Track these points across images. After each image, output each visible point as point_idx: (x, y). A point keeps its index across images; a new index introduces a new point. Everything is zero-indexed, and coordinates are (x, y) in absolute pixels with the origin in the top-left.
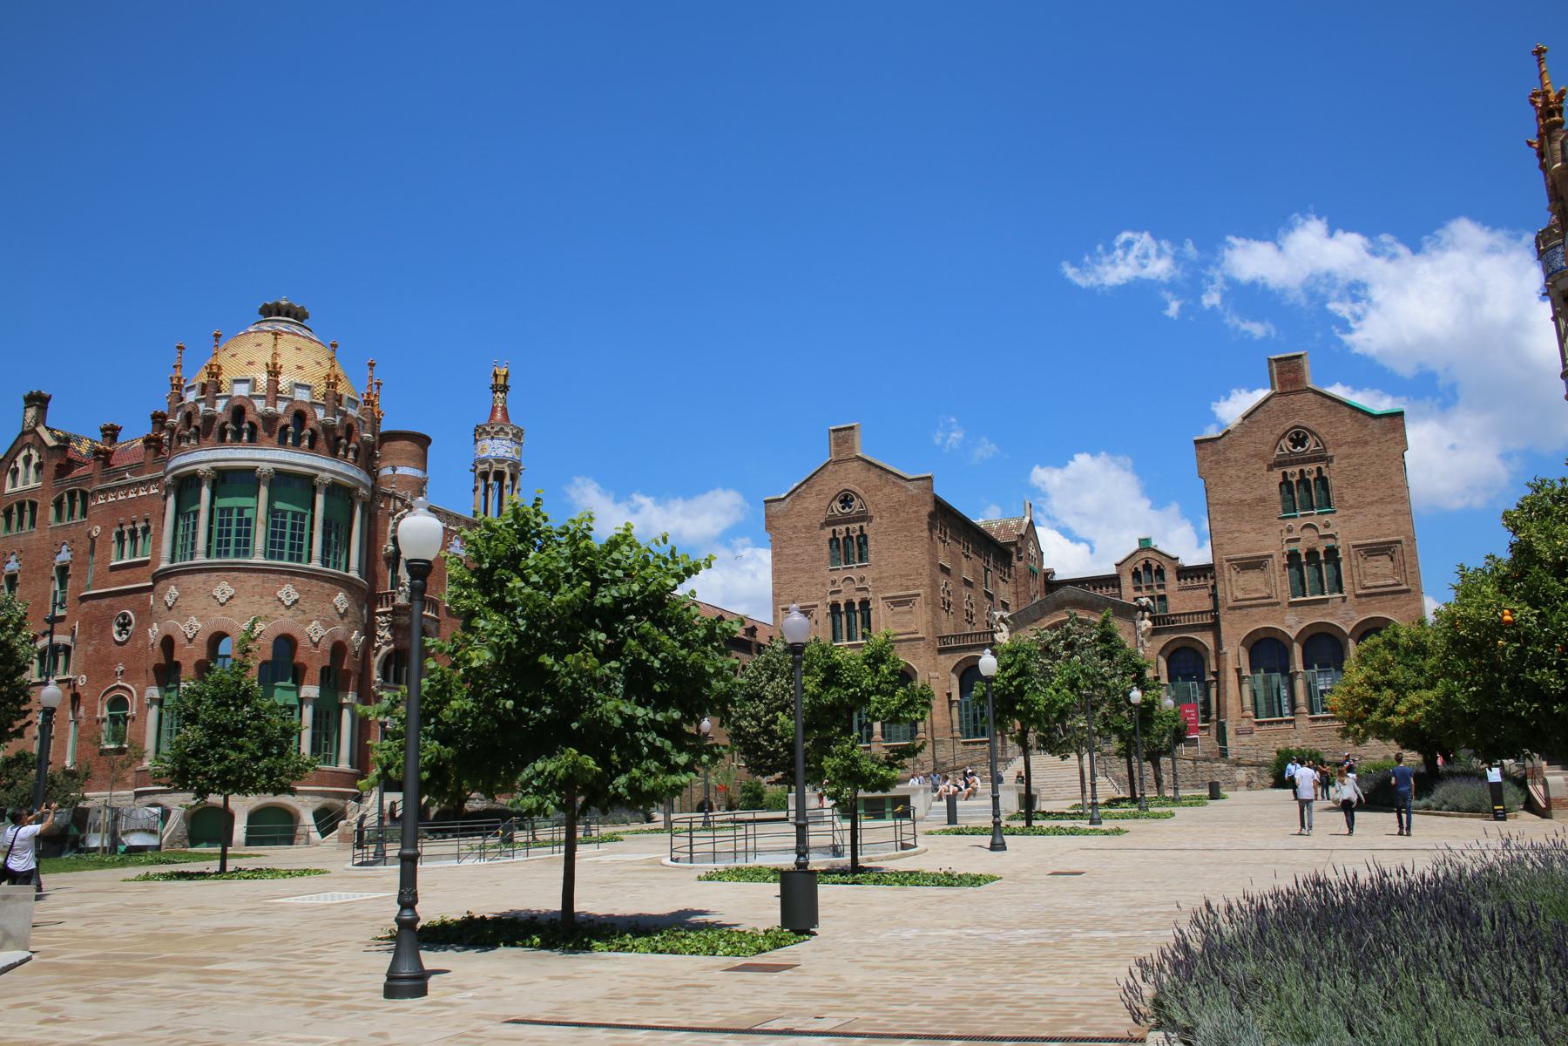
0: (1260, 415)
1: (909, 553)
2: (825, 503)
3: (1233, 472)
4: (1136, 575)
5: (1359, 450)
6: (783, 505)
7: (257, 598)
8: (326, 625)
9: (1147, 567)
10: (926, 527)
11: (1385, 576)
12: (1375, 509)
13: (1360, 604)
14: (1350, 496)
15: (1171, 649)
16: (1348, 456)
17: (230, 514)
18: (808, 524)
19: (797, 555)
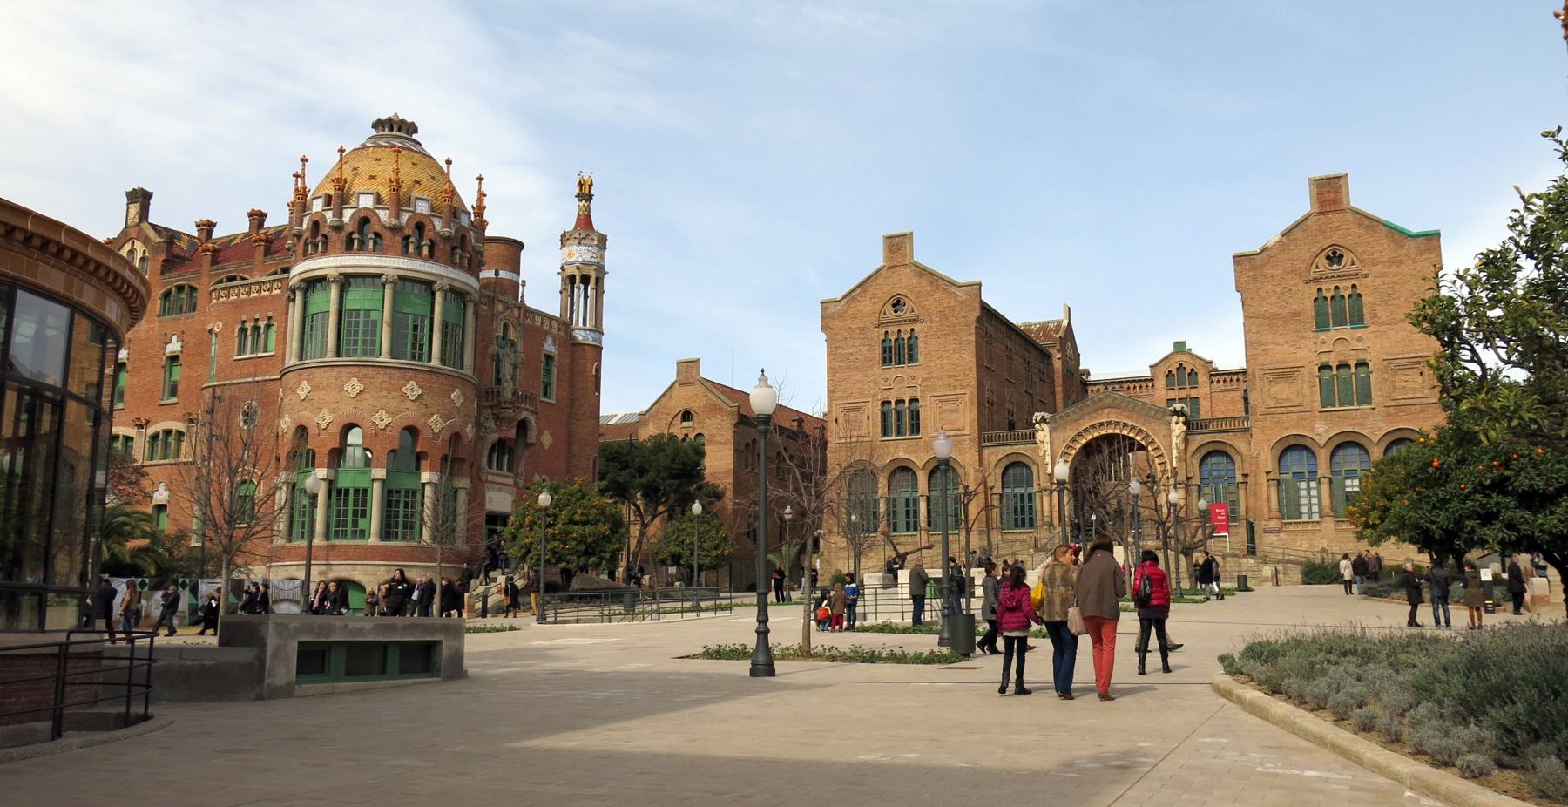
0: (1298, 233)
2: (879, 306)
4: (1169, 375)
5: (1394, 269)
7: (385, 393)
8: (445, 418)
9: (1181, 367)
10: (973, 331)
11: (1414, 390)
13: (1388, 415)
15: (1204, 451)
17: (357, 316)
18: (862, 325)
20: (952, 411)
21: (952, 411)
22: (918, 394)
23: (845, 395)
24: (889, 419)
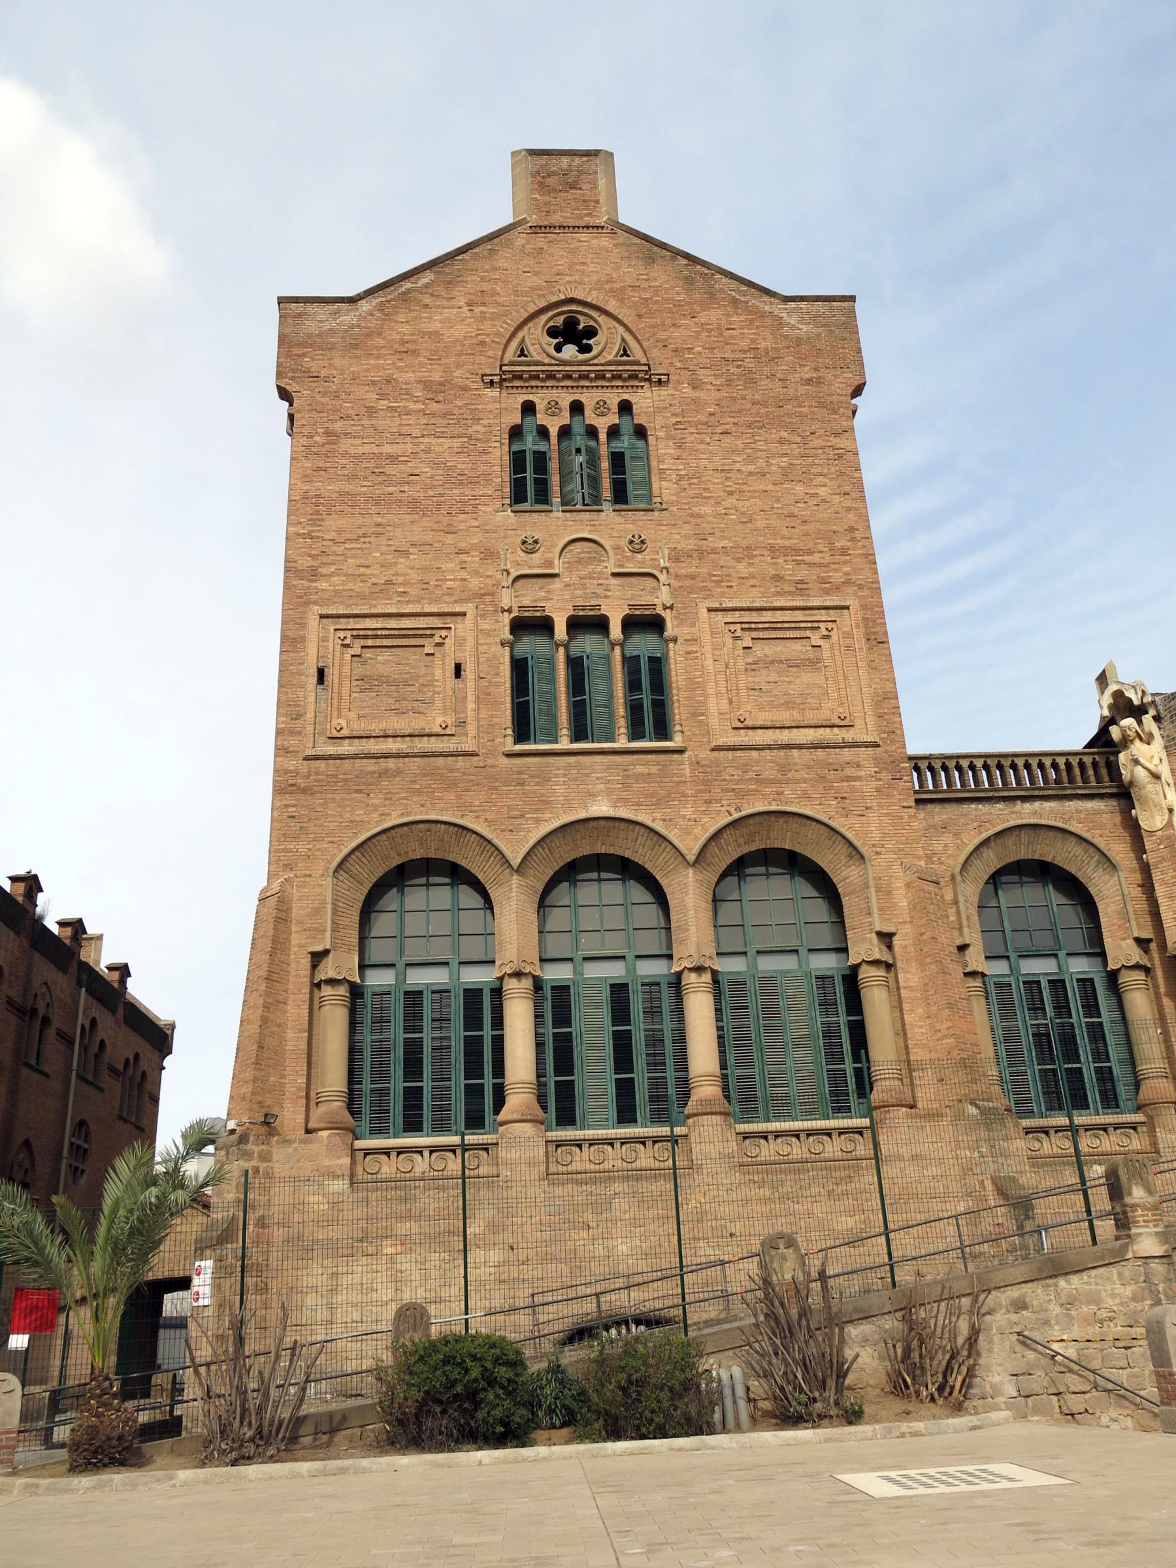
1: (799, 489)
2: (504, 327)
6: (349, 317)
18: (437, 376)
19: (393, 459)
20: (792, 664)
21: (792, 664)
22: (660, 597)
23: (358, 586)
24: (536, 684)
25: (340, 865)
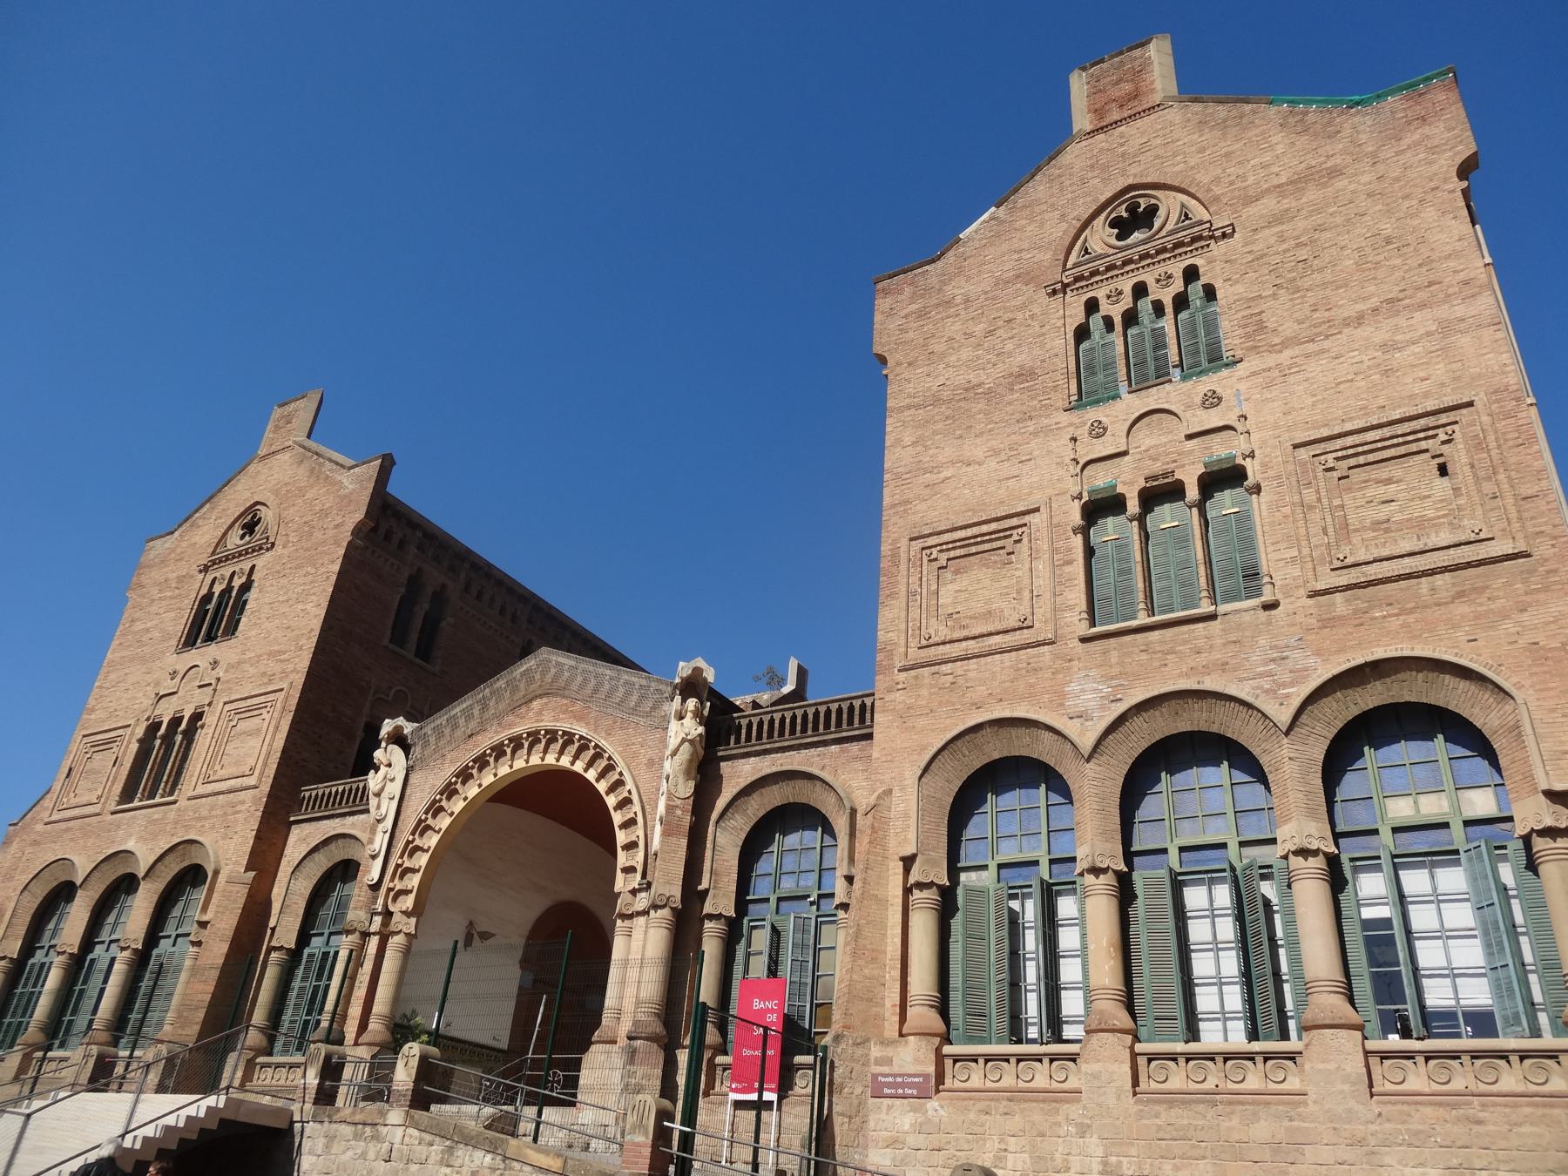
3: (957, 326)
12: (1369, 332)
13: (1327, 622)
14: (1282, 316)
16: (1277, 219)
25: (25, 888)
